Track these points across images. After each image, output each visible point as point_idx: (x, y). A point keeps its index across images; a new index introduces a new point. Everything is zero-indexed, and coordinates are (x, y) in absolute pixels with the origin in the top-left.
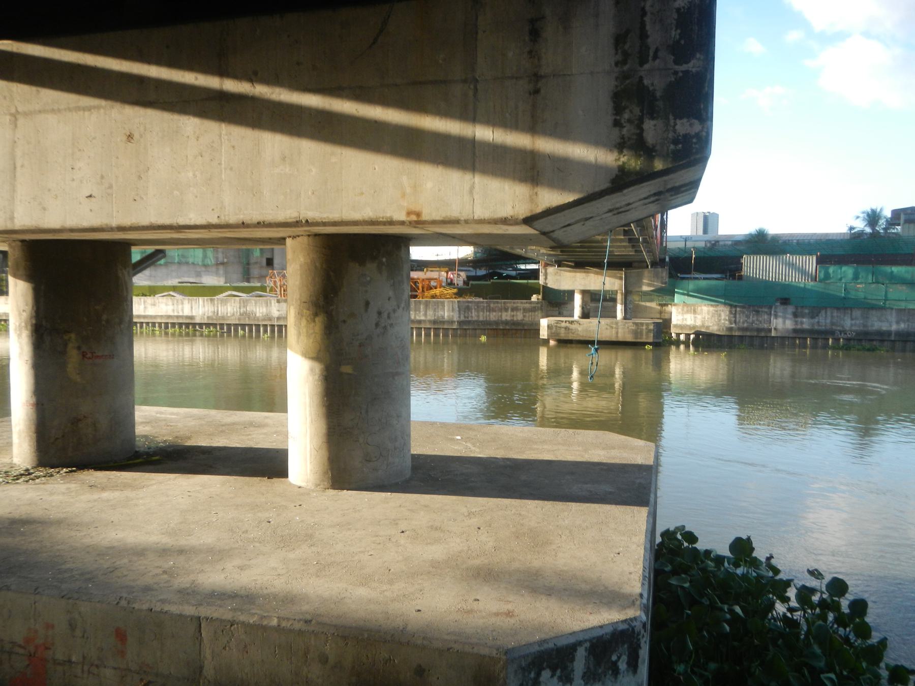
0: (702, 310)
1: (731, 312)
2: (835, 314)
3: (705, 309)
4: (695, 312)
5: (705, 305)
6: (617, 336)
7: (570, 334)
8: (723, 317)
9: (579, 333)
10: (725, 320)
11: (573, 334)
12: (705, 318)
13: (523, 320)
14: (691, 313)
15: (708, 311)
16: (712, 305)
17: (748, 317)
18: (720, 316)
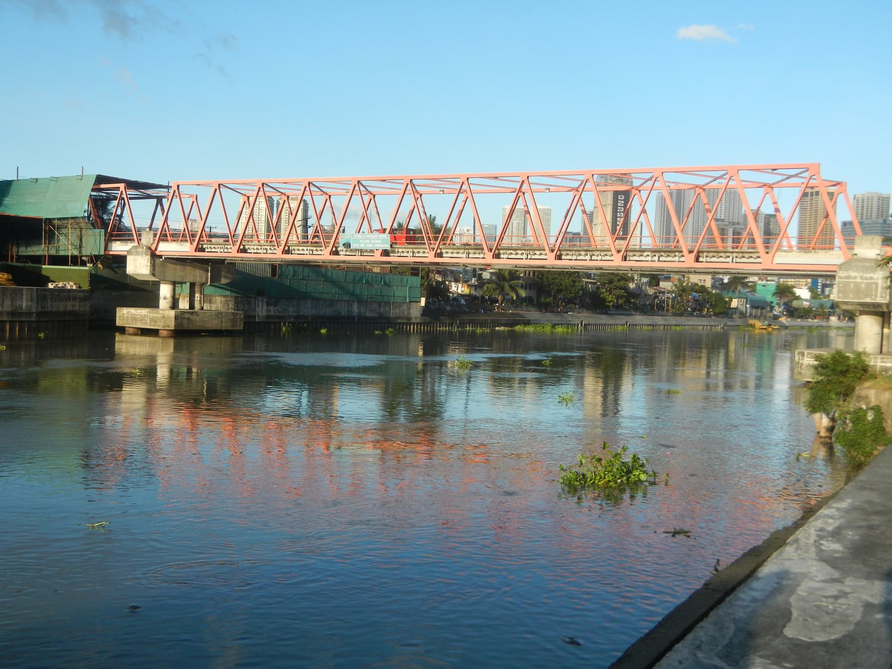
0: (216, 300)
1: (235, 303)
2: (286, 303)
3: (219, 299)
4: (210, 302)
5: (219, 296)
6: (222, 326)
7: (191, 325)
8: (230, 306)
9: (198, 324)
10: (232, 308)
11: (192, 324)
12: (218, 307)
13: (79, 310)
14: (207, 303)
15: (221, 301)
16: (224, 296)
17: (244, 306)
18: (229, 305)
